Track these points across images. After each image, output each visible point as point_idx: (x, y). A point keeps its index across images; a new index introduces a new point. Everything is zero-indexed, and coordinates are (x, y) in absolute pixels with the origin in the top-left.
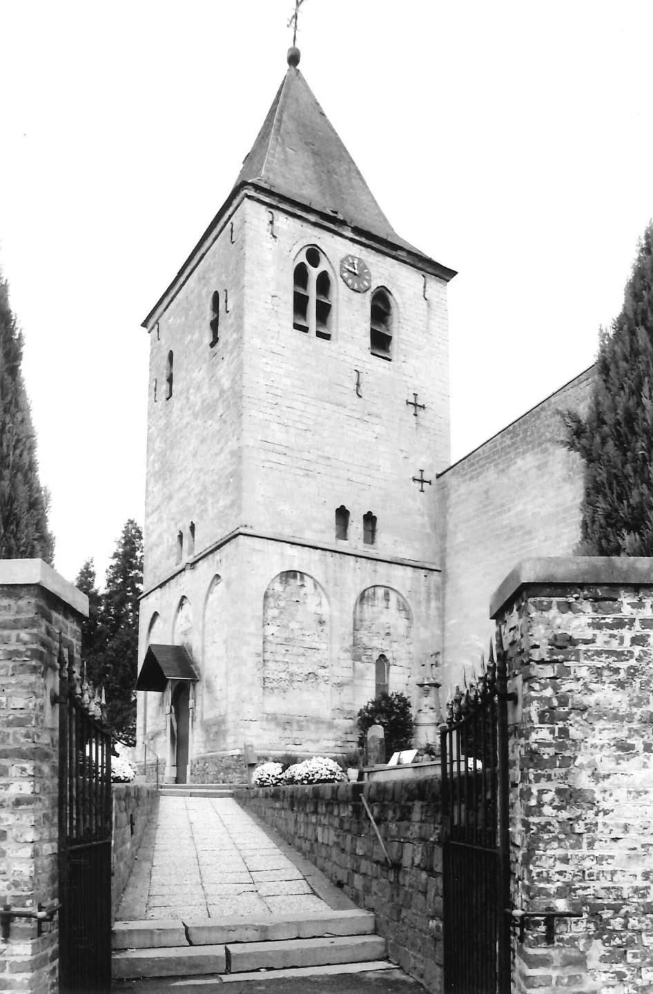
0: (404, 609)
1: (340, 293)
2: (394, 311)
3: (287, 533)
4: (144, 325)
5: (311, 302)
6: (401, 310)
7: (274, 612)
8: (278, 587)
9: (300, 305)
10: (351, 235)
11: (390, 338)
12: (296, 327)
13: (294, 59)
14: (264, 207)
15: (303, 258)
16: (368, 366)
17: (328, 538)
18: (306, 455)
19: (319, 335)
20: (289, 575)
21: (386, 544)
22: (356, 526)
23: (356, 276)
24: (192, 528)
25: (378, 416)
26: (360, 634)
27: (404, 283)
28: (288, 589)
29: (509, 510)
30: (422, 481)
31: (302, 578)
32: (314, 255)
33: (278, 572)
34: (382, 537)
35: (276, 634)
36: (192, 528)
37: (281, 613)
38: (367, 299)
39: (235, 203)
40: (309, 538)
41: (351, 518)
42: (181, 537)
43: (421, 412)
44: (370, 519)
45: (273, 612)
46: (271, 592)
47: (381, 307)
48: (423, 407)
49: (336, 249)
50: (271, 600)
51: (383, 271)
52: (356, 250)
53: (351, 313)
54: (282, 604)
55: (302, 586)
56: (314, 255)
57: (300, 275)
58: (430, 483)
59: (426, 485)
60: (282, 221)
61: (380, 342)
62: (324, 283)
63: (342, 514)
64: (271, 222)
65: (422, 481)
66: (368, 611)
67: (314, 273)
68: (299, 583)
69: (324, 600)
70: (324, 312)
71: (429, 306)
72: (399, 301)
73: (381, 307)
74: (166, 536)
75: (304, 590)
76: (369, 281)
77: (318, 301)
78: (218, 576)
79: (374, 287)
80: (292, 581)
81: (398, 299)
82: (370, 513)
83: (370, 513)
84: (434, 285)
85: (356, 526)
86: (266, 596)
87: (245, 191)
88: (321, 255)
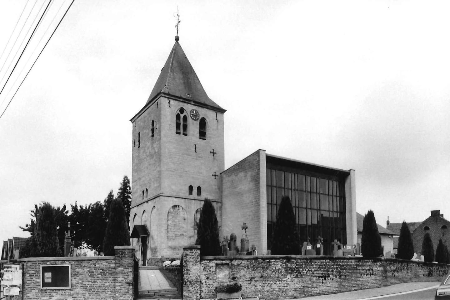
1: (190, 120)
2: (207, 124)
3: (174, 194)
4: (131, 120)
5: (181, 126)
8: (172, 210)
10: (193, 103)
11: (206, 133)
12: (177, 133)
13: (177, 39)
14: (167, 99)
15: (179, 112)
17: (187, 195)
19: (184, 134)
20: (175, 207)
22: (195, 191)
23: (195, 116)
24: (147, 190)
25: (201, 158)
27: (209, 115)
28: (175, 210)
29: (238, 187)
30: (215, 176)
31: (179, 207)
32: (182, 110)
33: (172, 206)
35: (171, 223)
36: (147, 190)
37: (173, 217)
38: (198, 122)
39: (158, 97)
40: (181, 195)
41: (193, 188)
42: (143, 192)
43: (215, 155)
44: (199, 189)
45: (170, 217)
46: (169, 212)
47: (203, 124)
48: (216, 153)
49: (189, 108)
50: (170, 214)
51: (203, 112)
52: (195, 108)
53: (194, 127)
54: (173, 215)
55: (179, 209)
56: (182, 110)
57: (178, 117)
58: (218, 176)
59: (216, 177)
60: (172, 102)
61: (203, 135)
62: (185, 118)
63: (191, 188)
64: (169, 103)
65: (215, 176)
67: (182, 116)
69: (185, 213)
70: (185, 127)
71: (218, 121)
74: (139, 191)
76: (199, 117)
77: (183, 124)
78: (154, 206)
79: (200, 118)
80: (176, 208)
82: (199, 186)
83: (199, 186)
84: (219, 115)
85: (195, 191)
86: (168, 213)
87: (161, 95)
88: (184, 110)
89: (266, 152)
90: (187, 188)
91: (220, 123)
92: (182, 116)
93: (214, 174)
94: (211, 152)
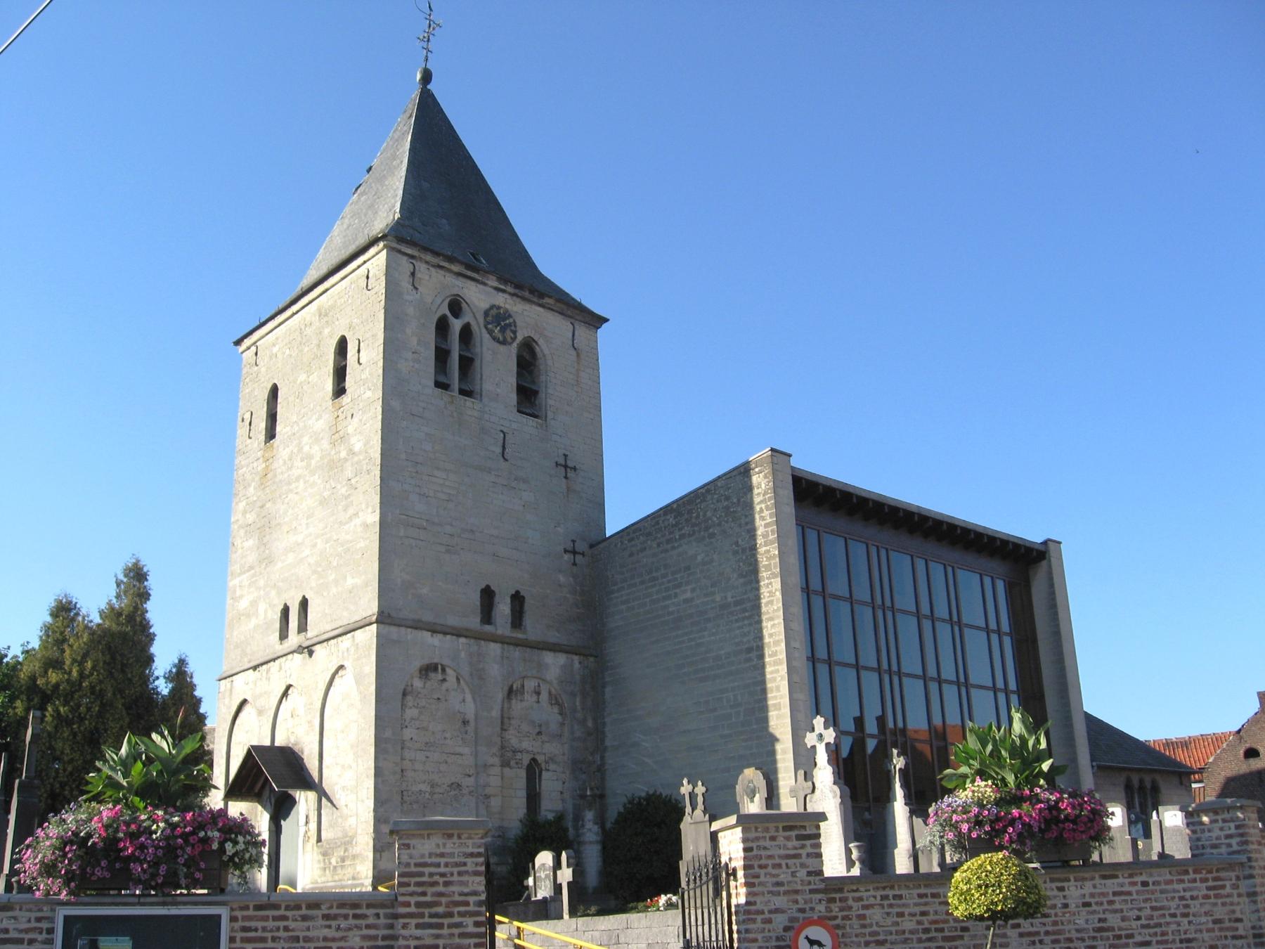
0: (557, 703)
1: (485, 345)
2: (541, 361)
3: (428, 617)
6: (550, 363)
7: (415, 712)
8: (418, 683)
9: (442, 356)
10: (496, 284)
12: (438, 384)
14: (405, 258)
16: (514, 426)
17: (474, 622)
18: (448, 529)
19: (463, 392)
20: (428, 670)
21: (534, 628)
22: (503, 608)
25: (525, 481)
26: (508, 735)
28: (429, 683)
29: (676, 595)
30: (574, 553)
31: (444, 670)
32: (456, 306)
34: (528, 620)
35: (415, 738)
37: (421, 713)
38: (514, 348)
40: (453, 621)
41: (497, 599)
42: (286, 611)
43: (571, 474)
44: (518, 600)
45: (411, 713)
46: (409, 689)
47: (528, 361)
48: (575, 469)
49: (480, 296)
50: (409, 698)
51: (530, 318)
53: (497, 368)
54: (423, 703)
55: (444, 680)
56: (456, 306)
57: (442, 327)
58: (583, 554)
61: (528, 397)
62: (466, 333)
63: (488, 595)
64: (413, 274)
65: (574, 553)
66: (517, 706)
67: (456, 325)
68: (440, 677)
69: (469, 697)
70: (467, 364)
71: (578, 355)
72: (546, 352)
73: (528, 361)
74: (262, 607)
75: (445, 685)
76: (514, 332)
77: (461, 357)
79: (520, 338)
80: (432, 675)
81: (543, 347)
82: (518, 592)
84: (582, 331)
85: (503, 608)
86: (404, 694)
88: (464, 305)
89: (794, 462)
90: (475, 598)
91: (587, 360)
92: (456, 325)
93: (569, 546)
94: (557, 464)
